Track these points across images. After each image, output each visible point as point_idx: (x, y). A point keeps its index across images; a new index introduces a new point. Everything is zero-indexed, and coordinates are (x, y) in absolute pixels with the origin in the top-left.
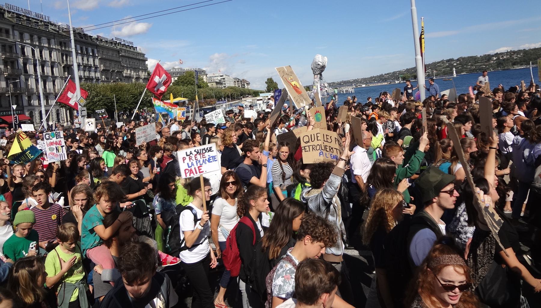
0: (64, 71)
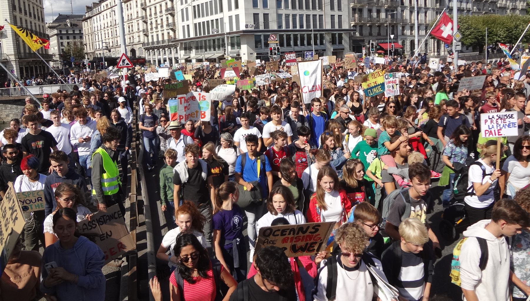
0: (437, 3)
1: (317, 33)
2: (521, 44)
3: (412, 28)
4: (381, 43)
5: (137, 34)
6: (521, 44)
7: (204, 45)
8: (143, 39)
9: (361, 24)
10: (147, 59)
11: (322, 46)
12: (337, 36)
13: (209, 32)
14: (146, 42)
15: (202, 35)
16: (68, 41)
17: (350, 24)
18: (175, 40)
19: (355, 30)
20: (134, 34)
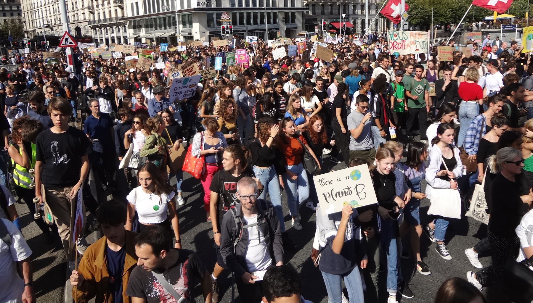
1: (270, 11)
2: (464, 24)
3: (363, 8)
4: (333, 22)
5: (82, 12)
6: (464, 24)
7: (154, 23)
8: (88, 16)
9: (313, 3)
10: (93, 37)
11: (275, 25)
12: (290, 14)
13: (159, 10)
14: (92, 19)
15: (152, 13)
16: (5, 18)
17: (303, 3)
18: (123, 18)
19: (308, 9)
20: (79, 11)
